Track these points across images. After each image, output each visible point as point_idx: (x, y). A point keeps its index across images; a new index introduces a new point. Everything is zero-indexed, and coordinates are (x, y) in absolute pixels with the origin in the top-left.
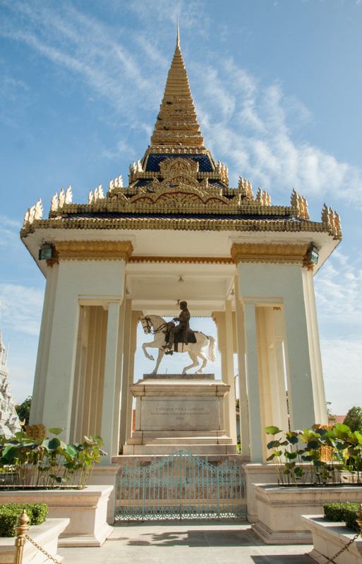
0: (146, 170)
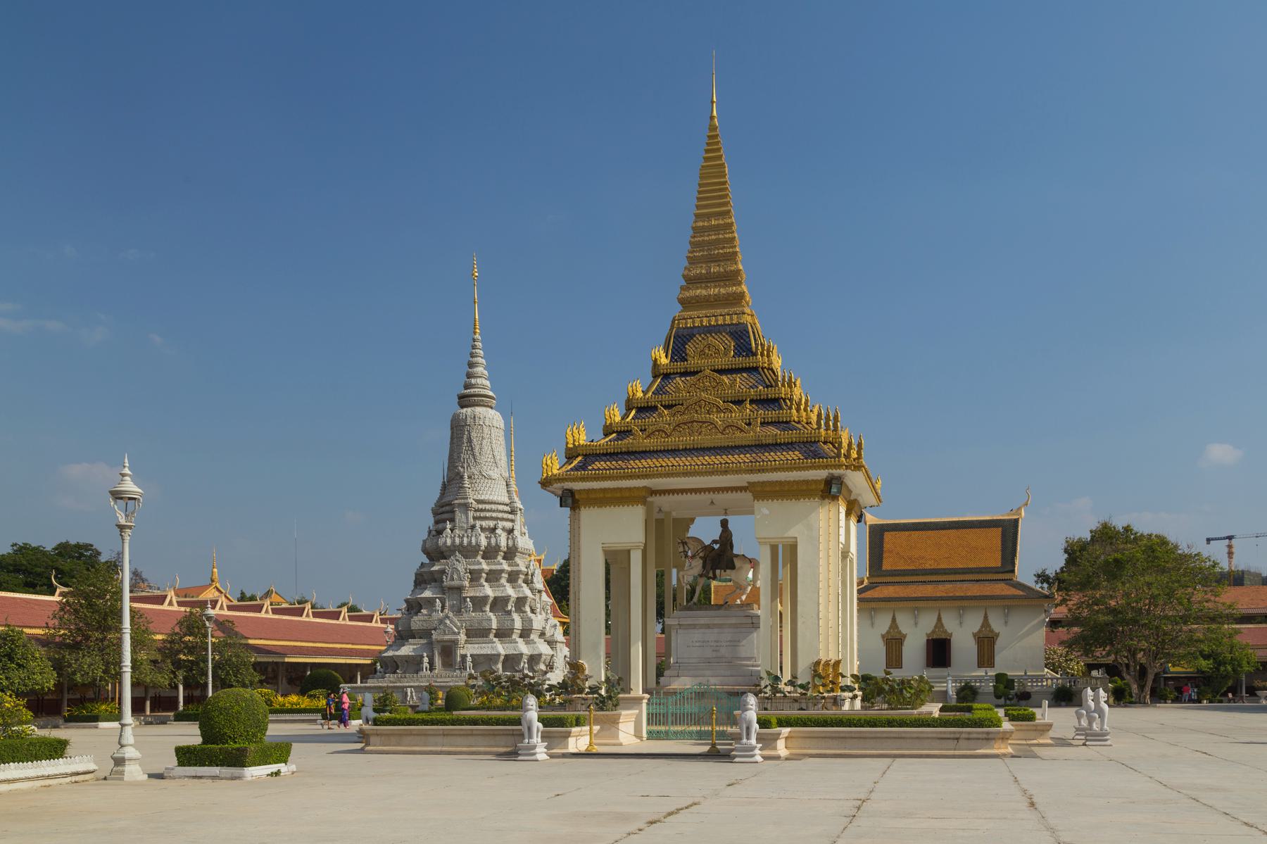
0: (671, 361)
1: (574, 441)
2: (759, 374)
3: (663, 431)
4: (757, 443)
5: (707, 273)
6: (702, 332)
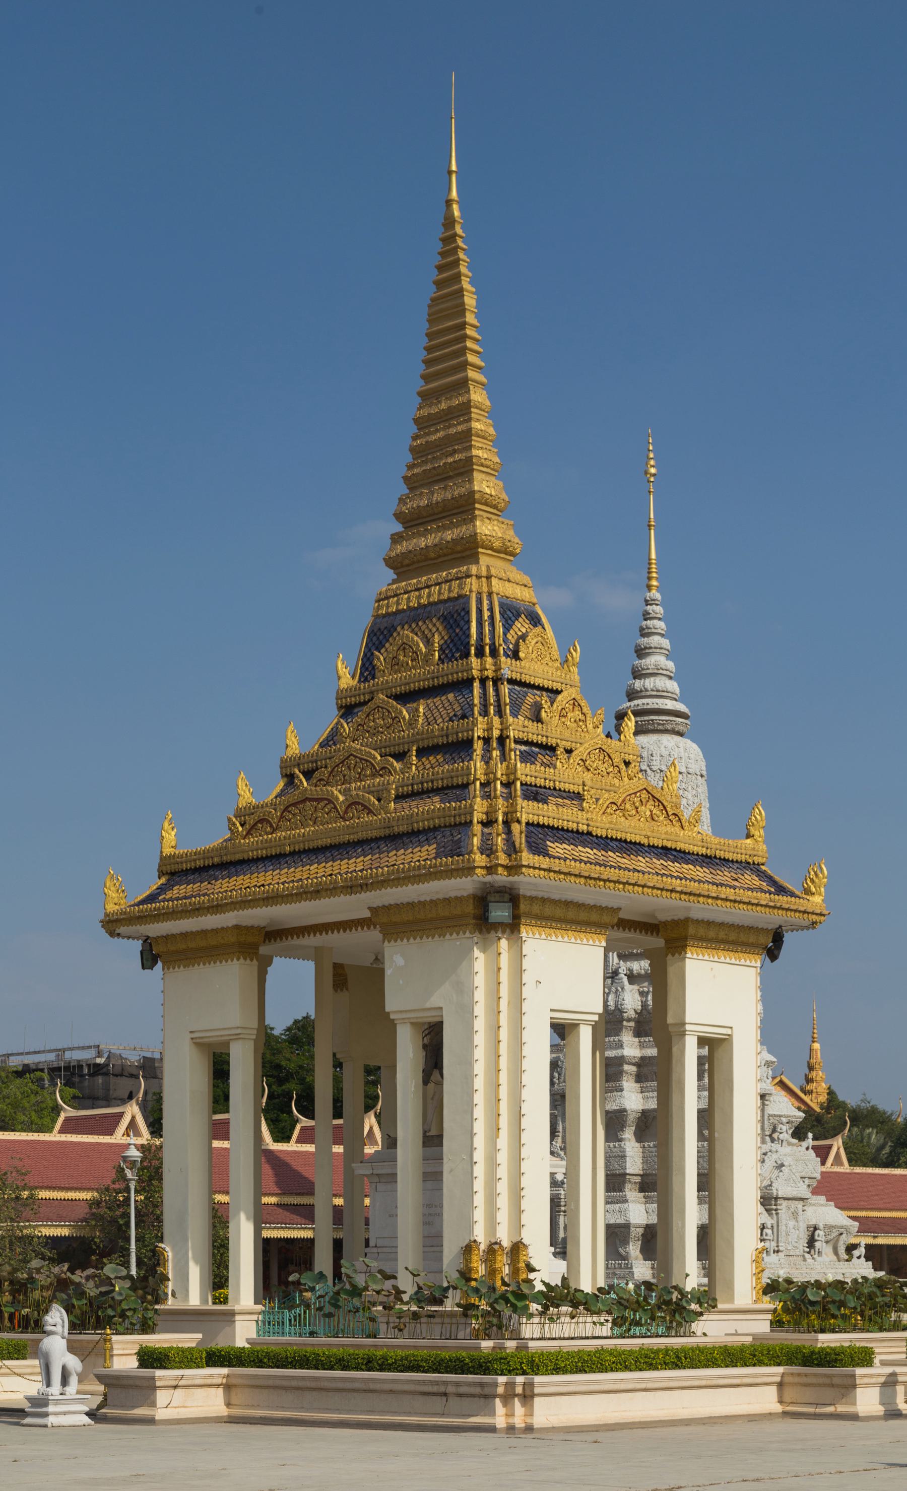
0: (359, 681)
4: (387, 832)
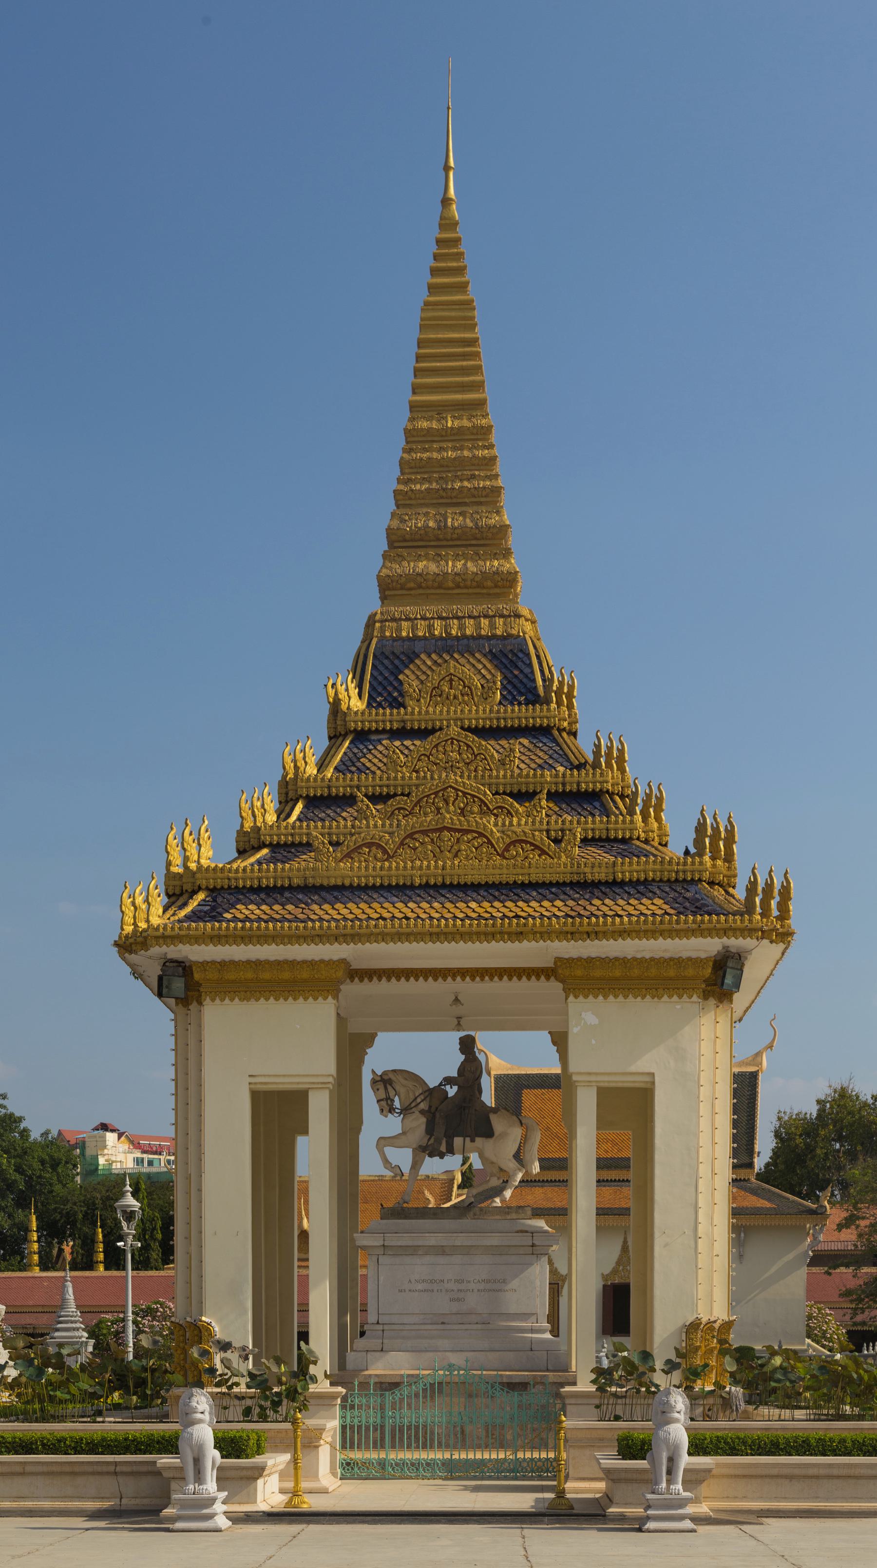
0: (369, 705)
1: (186, 859)
2: (555, 740)
3: (379, 846)
4: (575, 878)
5: (439, 528)
6: (433, 648)
